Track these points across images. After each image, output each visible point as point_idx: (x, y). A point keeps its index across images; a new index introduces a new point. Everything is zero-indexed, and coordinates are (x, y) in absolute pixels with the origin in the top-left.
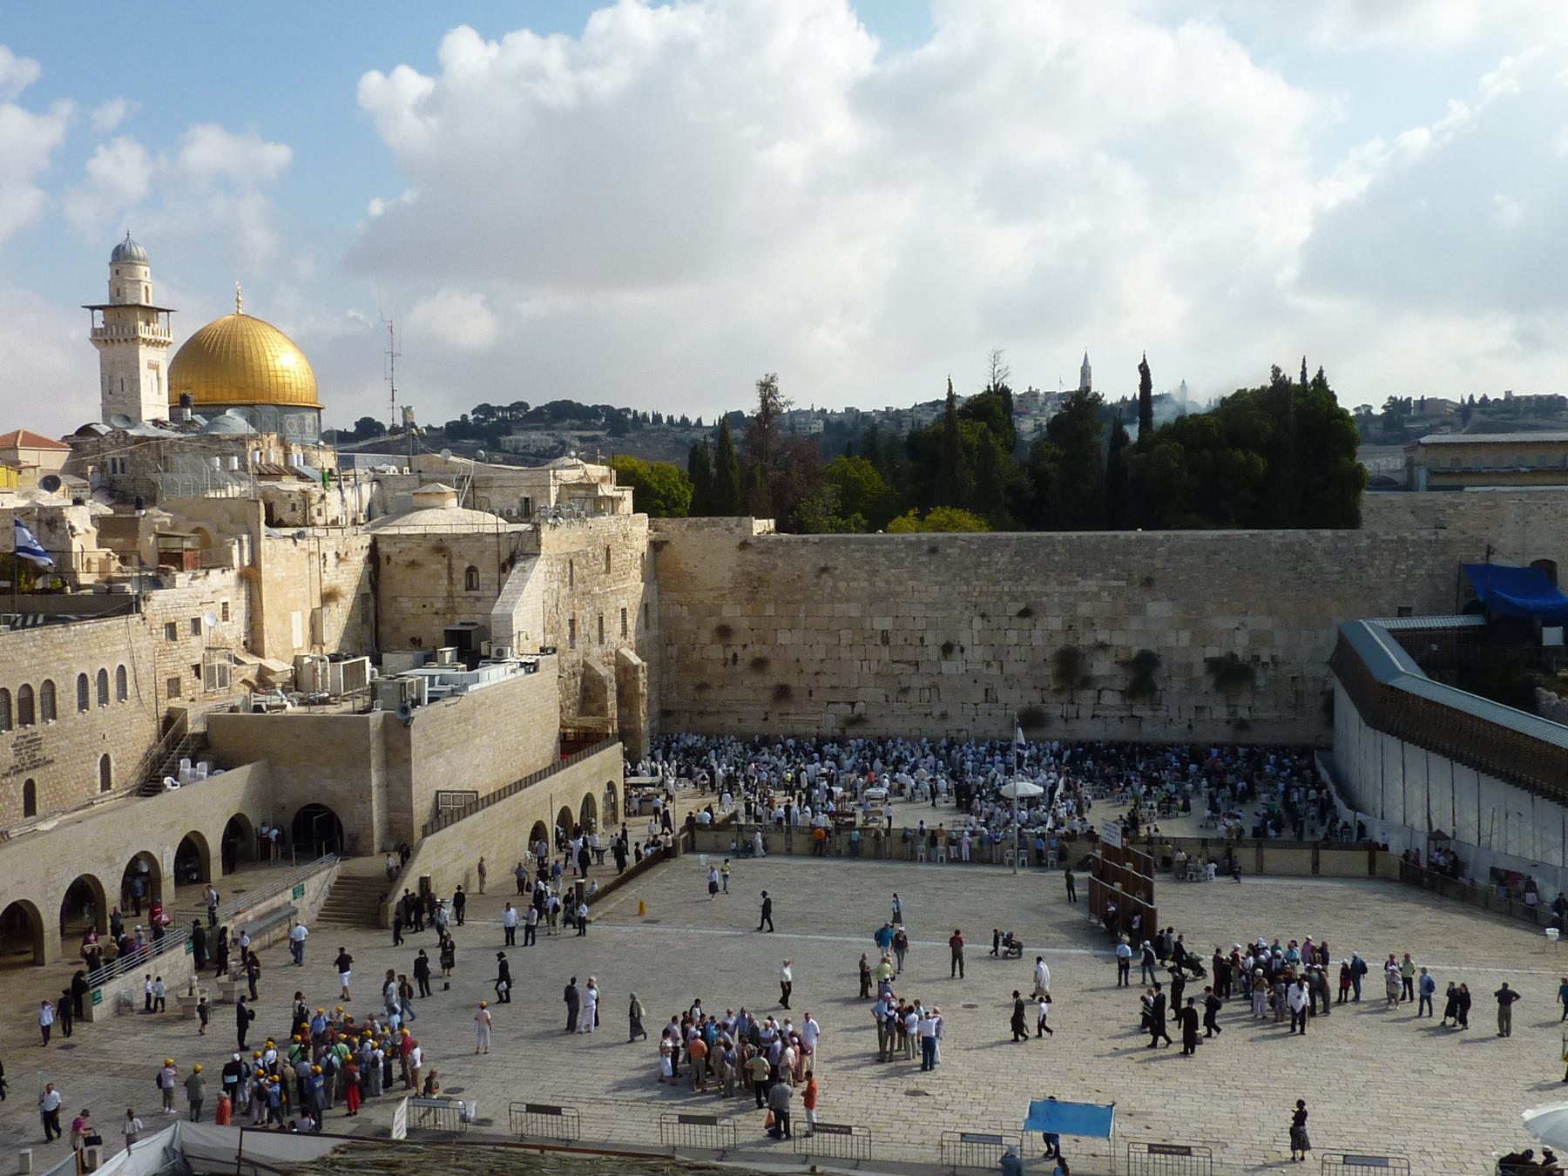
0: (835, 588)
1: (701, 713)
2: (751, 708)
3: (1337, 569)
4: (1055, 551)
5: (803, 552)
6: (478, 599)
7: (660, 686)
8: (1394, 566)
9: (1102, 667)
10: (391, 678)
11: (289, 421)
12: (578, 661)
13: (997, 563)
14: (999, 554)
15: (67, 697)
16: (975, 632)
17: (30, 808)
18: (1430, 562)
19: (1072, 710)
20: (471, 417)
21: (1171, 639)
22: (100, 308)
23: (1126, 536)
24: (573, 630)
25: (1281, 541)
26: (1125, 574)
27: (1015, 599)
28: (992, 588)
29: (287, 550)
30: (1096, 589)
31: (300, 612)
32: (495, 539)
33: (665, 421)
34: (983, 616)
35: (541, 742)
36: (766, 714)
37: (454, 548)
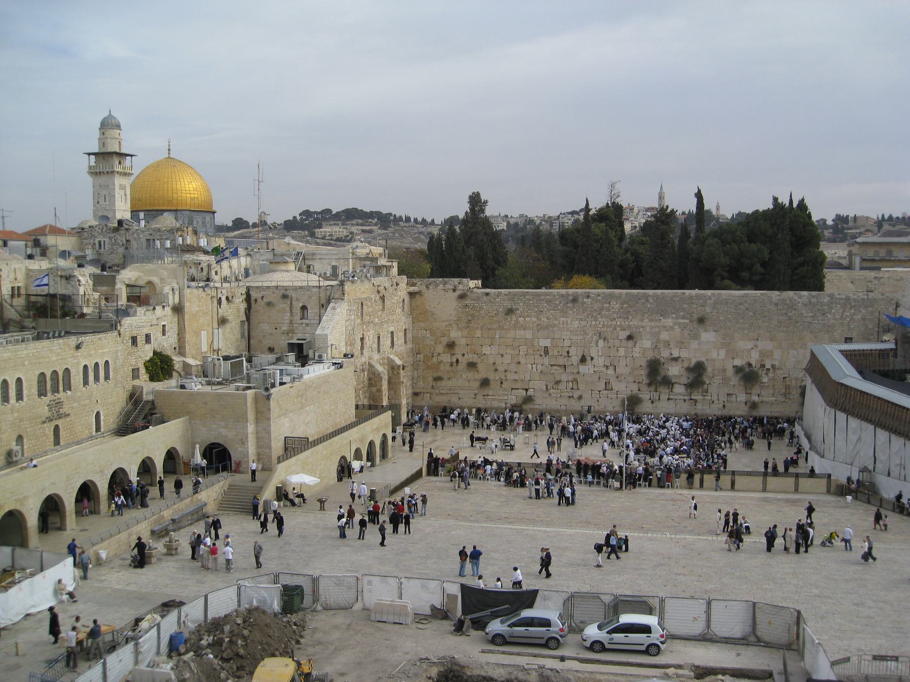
0: (517, 321)
2: (466, 392)
3: (812, 315)
4: (647, 301)
6: (307, 325)
7: (413, 378)
8: (843, 314)
9: (674, 371)
10: (258, 371)
12: (365, 363)
13: (613, 308)
14: (615, 303)
15: (77, 378)
17: (57, 441)
18: (863, 311)
19: (655, 396)
20: (298, 218)
21: (714, 355)
24: (362, 344)
25: (779, 298)
26: (688, 316)
27: (624, 330)
28: (610, 323)
29: (199, 295)
30: (671, 324)
31: (206, 332)
32: (318, 290)
33: (412, 220)
34: (605, 339)
35: (344, 410)
36: (475, 395)
37: (293, 295)
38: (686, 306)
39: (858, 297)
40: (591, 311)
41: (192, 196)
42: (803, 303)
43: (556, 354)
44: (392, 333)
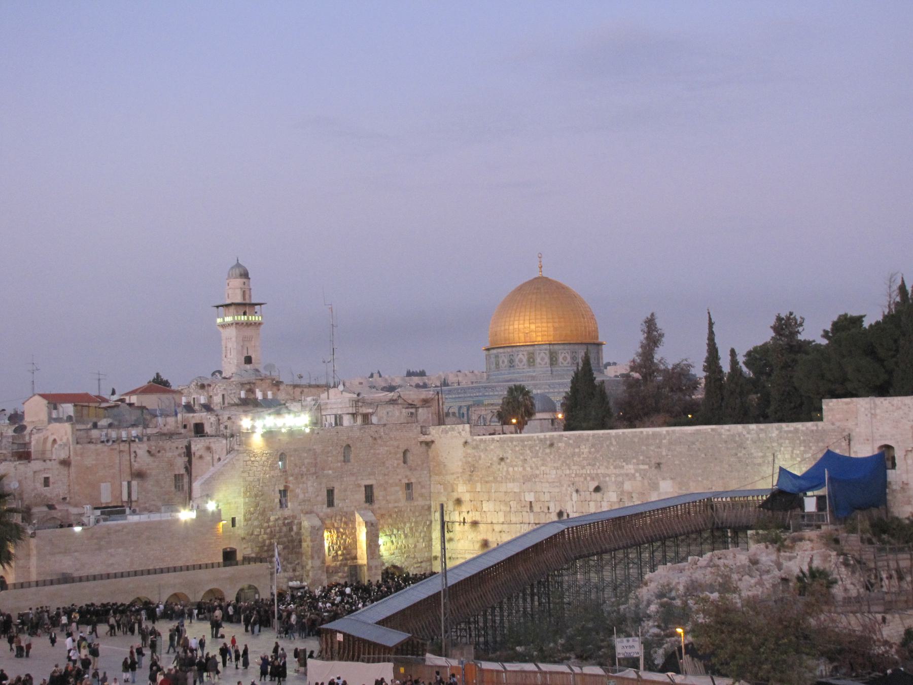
0: (507, 472)
3: (760, 454)
4: (611, 444)
11: (563, 355)
12: (294, 517)
14: (584, 447)
16: (574, 502)
18: (813, 448)
22: (222, 306)
23: (647, 432)
25: (728, 433)
26: (648, 460)
27: (593, 479)
30: (633, 471)
31: (109, 484)
34: (577, 491)
38: (644, 448)
39: (807, 429)
40: (564, 458)
41: (556, 325)
42: (752, 440)
43: (539, 511)
44: (366, 487)
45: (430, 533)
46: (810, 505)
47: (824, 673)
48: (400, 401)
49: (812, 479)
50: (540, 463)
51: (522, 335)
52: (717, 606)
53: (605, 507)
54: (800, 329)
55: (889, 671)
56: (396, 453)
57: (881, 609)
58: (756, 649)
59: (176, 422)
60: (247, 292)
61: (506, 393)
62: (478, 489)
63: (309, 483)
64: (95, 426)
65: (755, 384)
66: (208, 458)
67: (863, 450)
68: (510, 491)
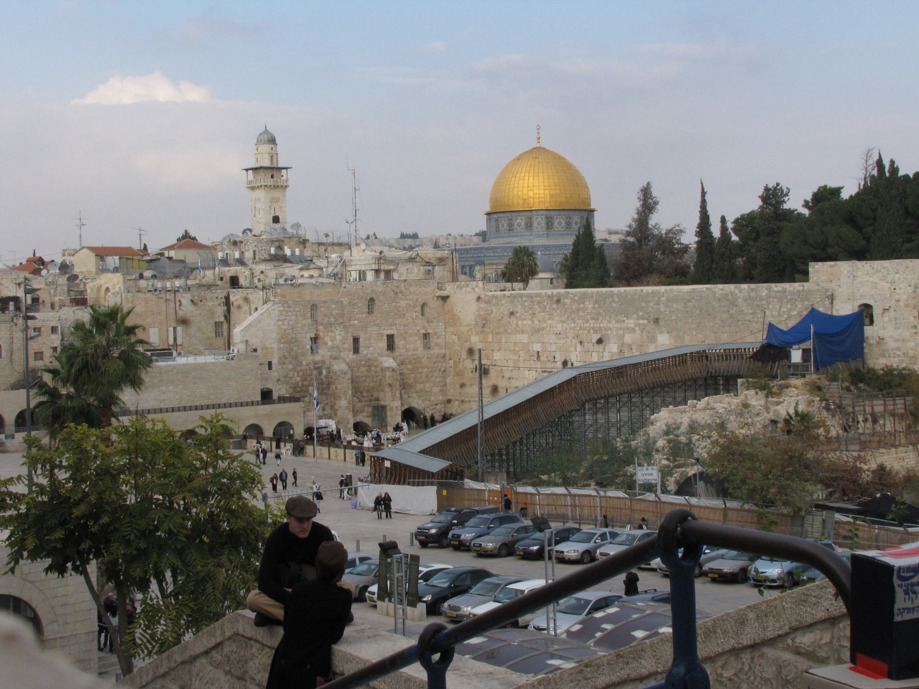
0: (517, 325)
1: (463, 401)
3: (750, 311)
4: (613, 300)
5: (503, 302)
8: (780, 309)
11: (558, 220)
12: (324, 362)
18: (799, 306)
25: (721, 292)
26: (647, 315)
27: (596, 332)
30: (633, 325)
31: (157, 329)
34: (581, 343)
38: (644, 304)
41: (552, 192)
43: (545, 360)
44: (388, 336)
45: (445, 378)
46: (796, 356)
47: (820, 498)
48: (418, 259)
49: (797, 335)
50: (547, 316)
51: (521, 202)
52: (730, 439)
53: (607, 357)
54: (786, 199)
55: (878, 495)
56: (415, 306)
57: (857, 447)
58: (765, 476)
59: (214, 274)
60: (275, 157)
61: (510, 254)
62: (490, 339)
63: (337, 332)
64: (141, 276)
65: (741, 248)
66: (245, 308)
67: (844, 308)
68: (519, 341)
